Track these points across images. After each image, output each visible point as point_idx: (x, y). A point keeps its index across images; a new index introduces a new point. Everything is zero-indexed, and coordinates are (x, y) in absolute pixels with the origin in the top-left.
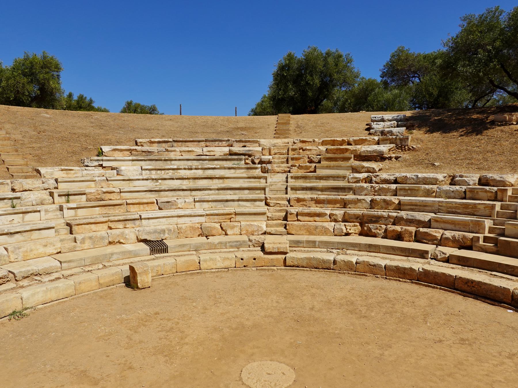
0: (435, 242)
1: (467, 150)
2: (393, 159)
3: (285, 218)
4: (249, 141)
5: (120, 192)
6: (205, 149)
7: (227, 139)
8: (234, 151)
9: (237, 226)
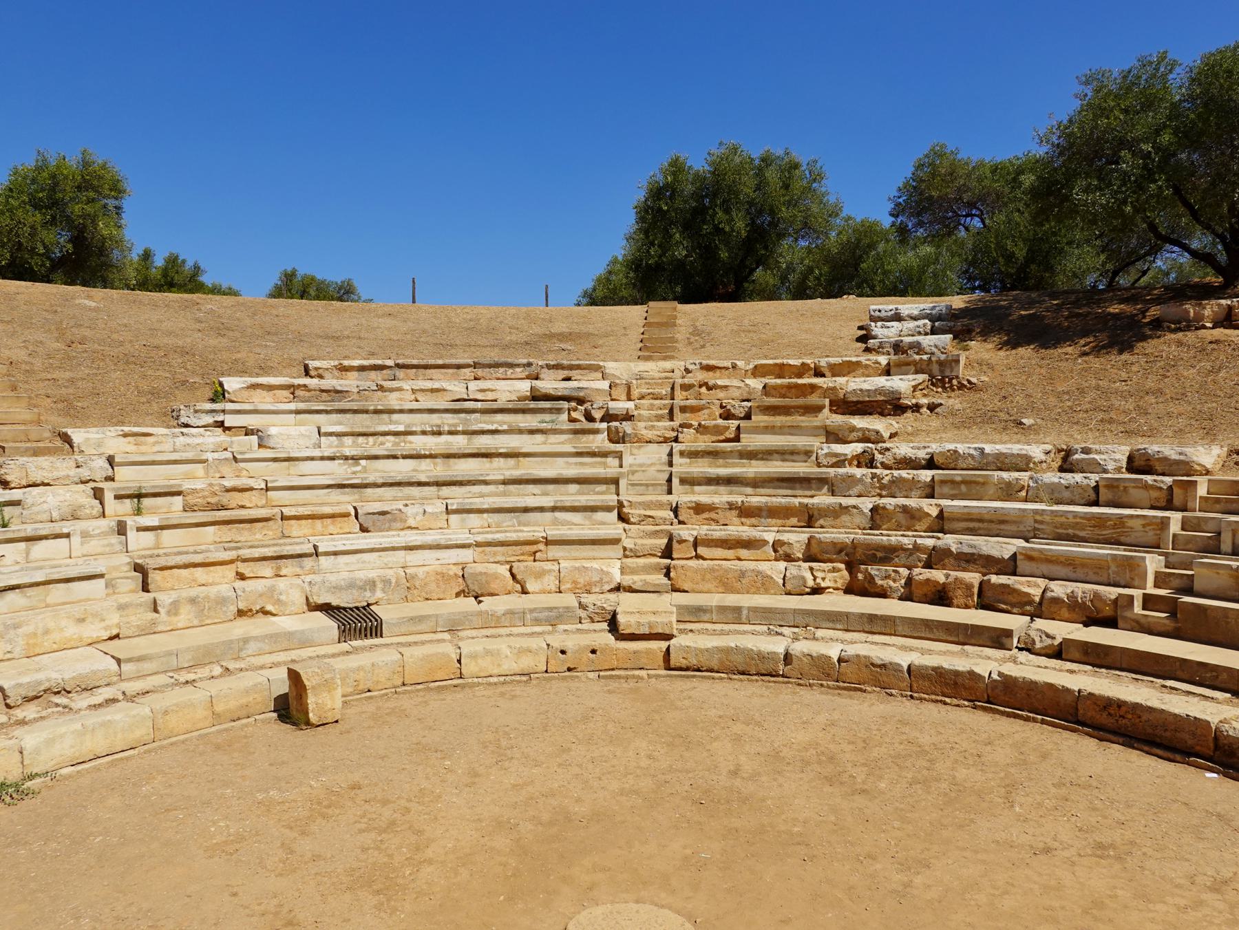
0: (1028, 608)
1: (1098, 388)
3: (667, 553)
4: (579, 367)
5: (267, 489)
6: (473, 385)
7: (525, 361)
8: (544, 391)
9: (550, 571)
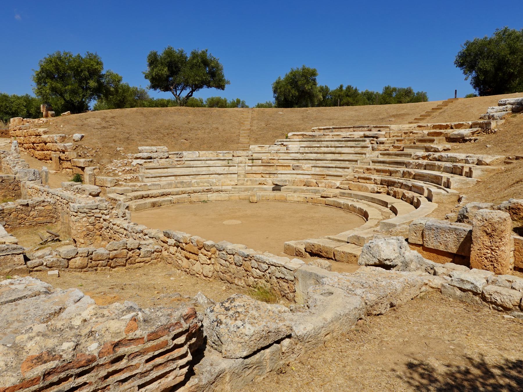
2: (473, 141)
4: (382, 127)
